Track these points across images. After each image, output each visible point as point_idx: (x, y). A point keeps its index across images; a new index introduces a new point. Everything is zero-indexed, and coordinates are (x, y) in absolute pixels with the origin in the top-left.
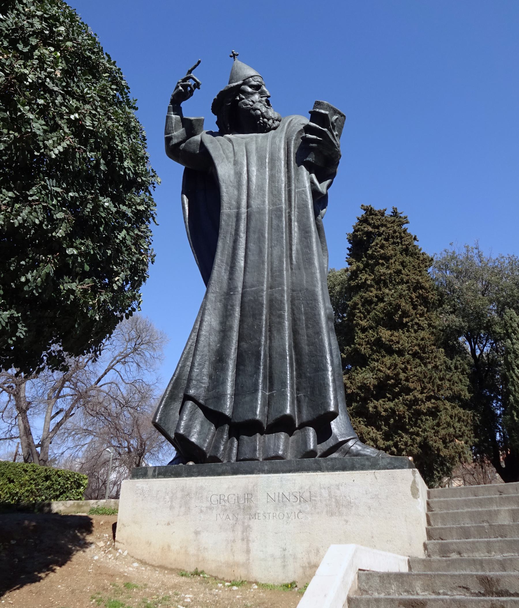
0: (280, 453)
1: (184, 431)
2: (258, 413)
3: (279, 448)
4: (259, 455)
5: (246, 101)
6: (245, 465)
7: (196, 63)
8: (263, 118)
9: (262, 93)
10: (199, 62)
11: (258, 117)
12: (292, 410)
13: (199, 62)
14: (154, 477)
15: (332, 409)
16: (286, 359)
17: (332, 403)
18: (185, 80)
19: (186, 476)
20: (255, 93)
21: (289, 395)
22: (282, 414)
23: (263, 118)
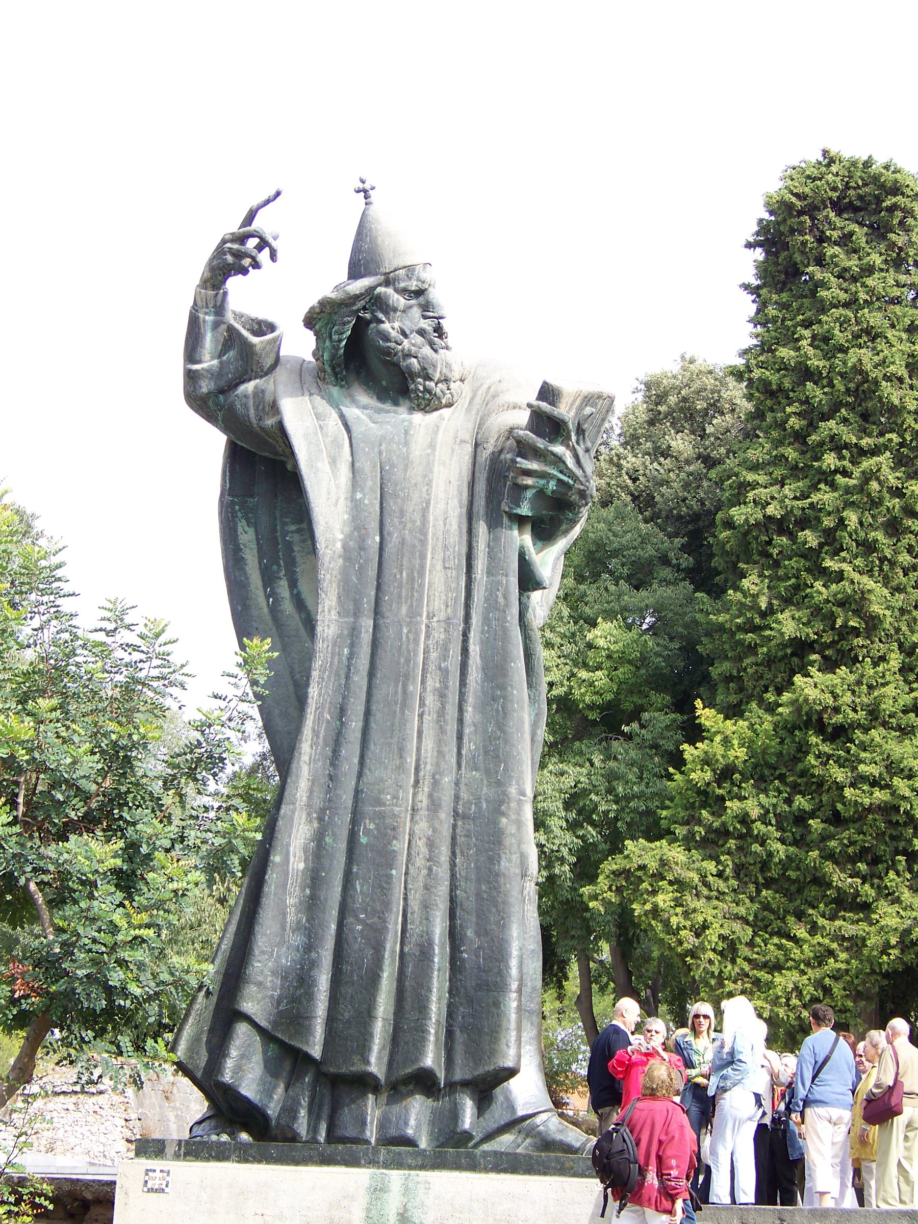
0: (410, 1132)
1: (232, 1078)
2: (373, 1060)
3: (406, 1124)
4: (371, 1134)
5: (386, 326)
6: (341, 1148)
7: (272, 193)
8: (425, 380)
9: (426, 307)
10: (278, 194)
11: (413, 375)
12: (437, 1058)
13: (278, 194)
14: (177, 1156)
15: (509, 1063)
16: (433, 961)
17: (512, 1052)
18: (242, 239)
19: (238, 1162)
20: (410, 307)
21: (432, 1031)
22: (415, 1067)
23: (425, 380)
